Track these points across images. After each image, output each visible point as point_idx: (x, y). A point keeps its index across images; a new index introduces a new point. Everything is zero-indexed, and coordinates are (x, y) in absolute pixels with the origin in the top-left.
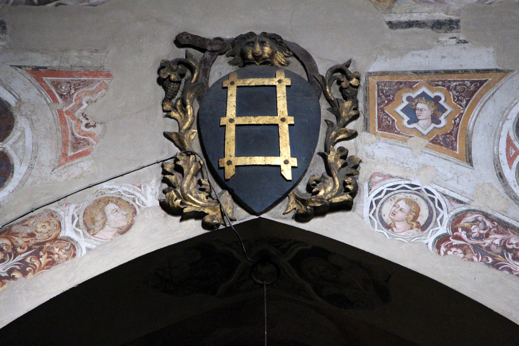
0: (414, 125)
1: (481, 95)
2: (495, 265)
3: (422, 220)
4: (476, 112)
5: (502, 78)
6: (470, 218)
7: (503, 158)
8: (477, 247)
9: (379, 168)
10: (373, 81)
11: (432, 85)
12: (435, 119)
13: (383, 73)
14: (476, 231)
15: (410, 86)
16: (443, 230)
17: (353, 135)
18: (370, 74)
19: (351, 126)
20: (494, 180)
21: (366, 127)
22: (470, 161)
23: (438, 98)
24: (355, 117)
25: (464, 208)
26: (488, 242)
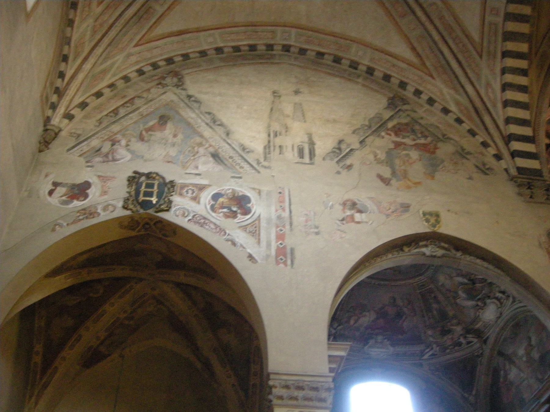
0: (187, 195)
1: (204, 190)
2: (201, 226)
3: (186, 215)
4: (202, 193)
5: (209, 187)
6: (197, 216)
7: (207, 203)
8: (198, 223)
9: (176, 203)
10: (179, 185)
11: (193, 187)
12: (192, 194)
13: (182, 183)
14: (198, 219)
15: (188, 186)
16: (190, 218)
17: (172, 196)
18: (179, 183)
19: (172, 194)
20: (203, 207)
21: (176, 194)
22: (199, 203)
23: (193, 190)
24: (173, 192)
25: (195, 214)
26: (200, 221)
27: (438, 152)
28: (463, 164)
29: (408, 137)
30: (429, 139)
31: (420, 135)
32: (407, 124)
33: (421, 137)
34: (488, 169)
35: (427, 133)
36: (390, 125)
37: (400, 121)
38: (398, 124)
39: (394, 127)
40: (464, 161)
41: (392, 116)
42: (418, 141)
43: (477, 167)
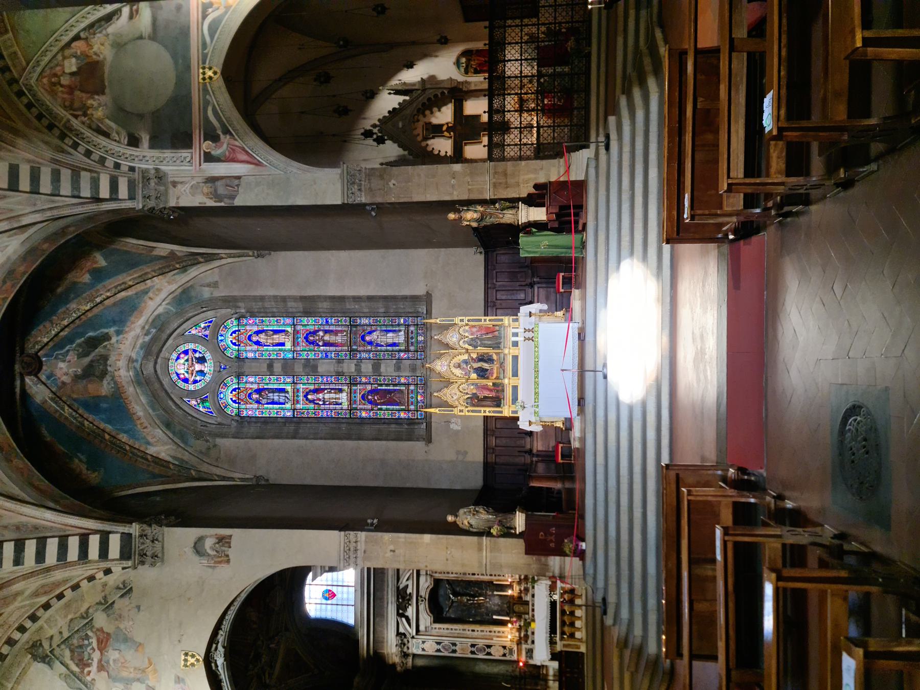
27: (105, 630)
28: (120, 609)
29: (89, 654)
30: (90, 633)
31: (86, 642)
32: (72, 651)
33: (88, 640)
34: (125, 587)
35: (82, 634)
36: (75, 669)
37: (69, 658)
38: (72, 659)
39: (77, 665)
40: (116, 606)
41: (62, 663)
42: (95, 645)
43: (122, 596)
